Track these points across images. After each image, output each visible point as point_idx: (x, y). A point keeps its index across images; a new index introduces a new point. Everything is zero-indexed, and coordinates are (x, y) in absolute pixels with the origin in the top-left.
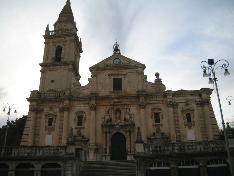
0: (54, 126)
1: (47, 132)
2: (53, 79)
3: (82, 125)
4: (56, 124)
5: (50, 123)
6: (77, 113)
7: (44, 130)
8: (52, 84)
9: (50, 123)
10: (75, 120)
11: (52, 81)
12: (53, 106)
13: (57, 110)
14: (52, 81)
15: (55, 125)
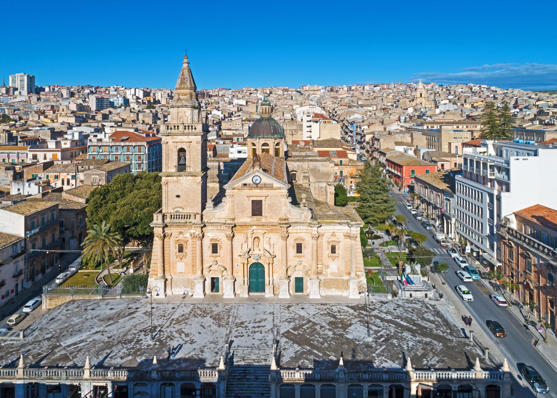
0: (186, 253)
1: (178, 259)
2: (179, 194)
3: (217, 253)
4: (188, 250)
5: (181, 249)
6: (211, 240)
7: (175, 257)
8: (177, 199)
9: (181, 249)
10: (209, 247)
11: (178, 196)
12: (182, 231)
13: (187, 235)
14: (178, 196)
15: (187, 251)
